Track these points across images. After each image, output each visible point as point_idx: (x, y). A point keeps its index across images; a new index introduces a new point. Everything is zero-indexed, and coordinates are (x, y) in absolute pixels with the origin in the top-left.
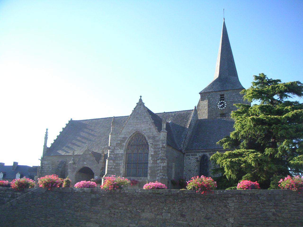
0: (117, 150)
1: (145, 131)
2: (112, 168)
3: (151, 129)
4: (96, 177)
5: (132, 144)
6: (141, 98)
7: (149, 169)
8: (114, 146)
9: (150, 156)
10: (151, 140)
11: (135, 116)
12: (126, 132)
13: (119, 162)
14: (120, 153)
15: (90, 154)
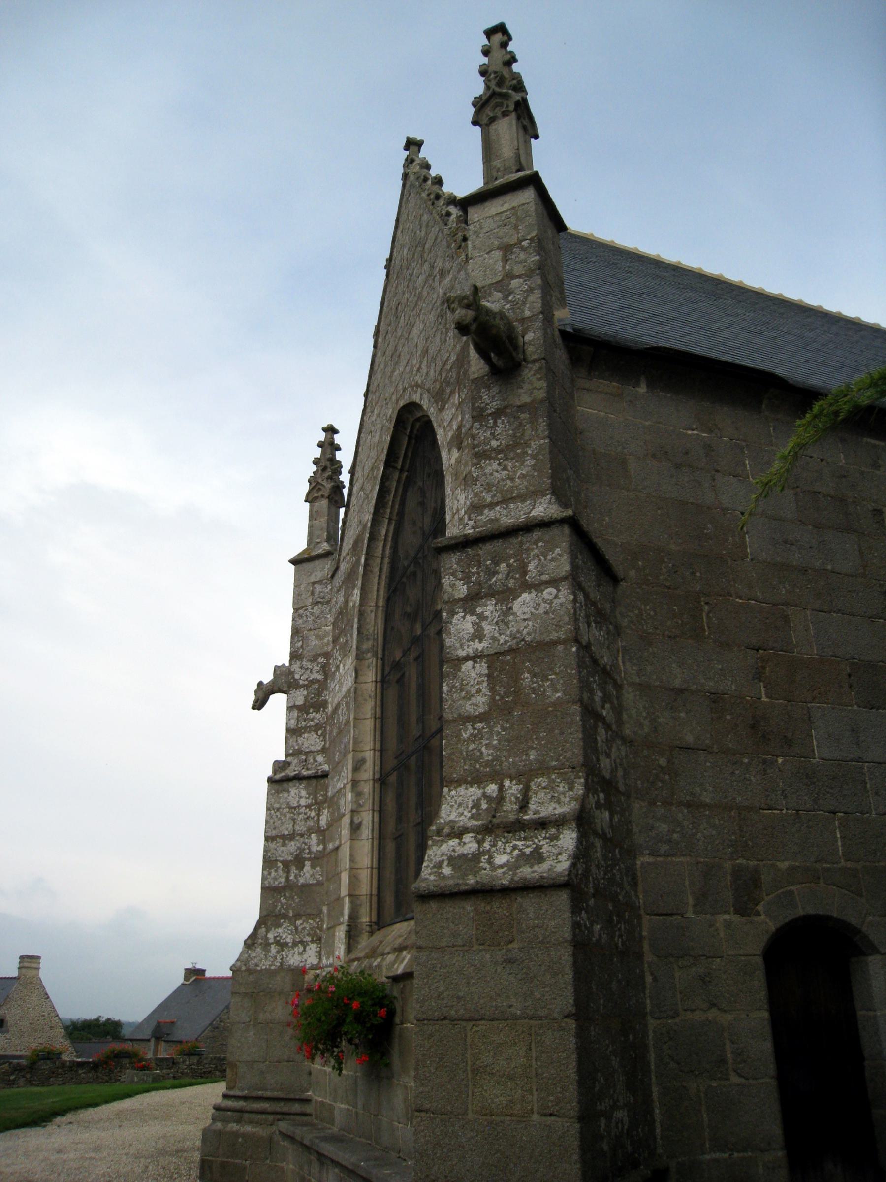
2: (299, 861)
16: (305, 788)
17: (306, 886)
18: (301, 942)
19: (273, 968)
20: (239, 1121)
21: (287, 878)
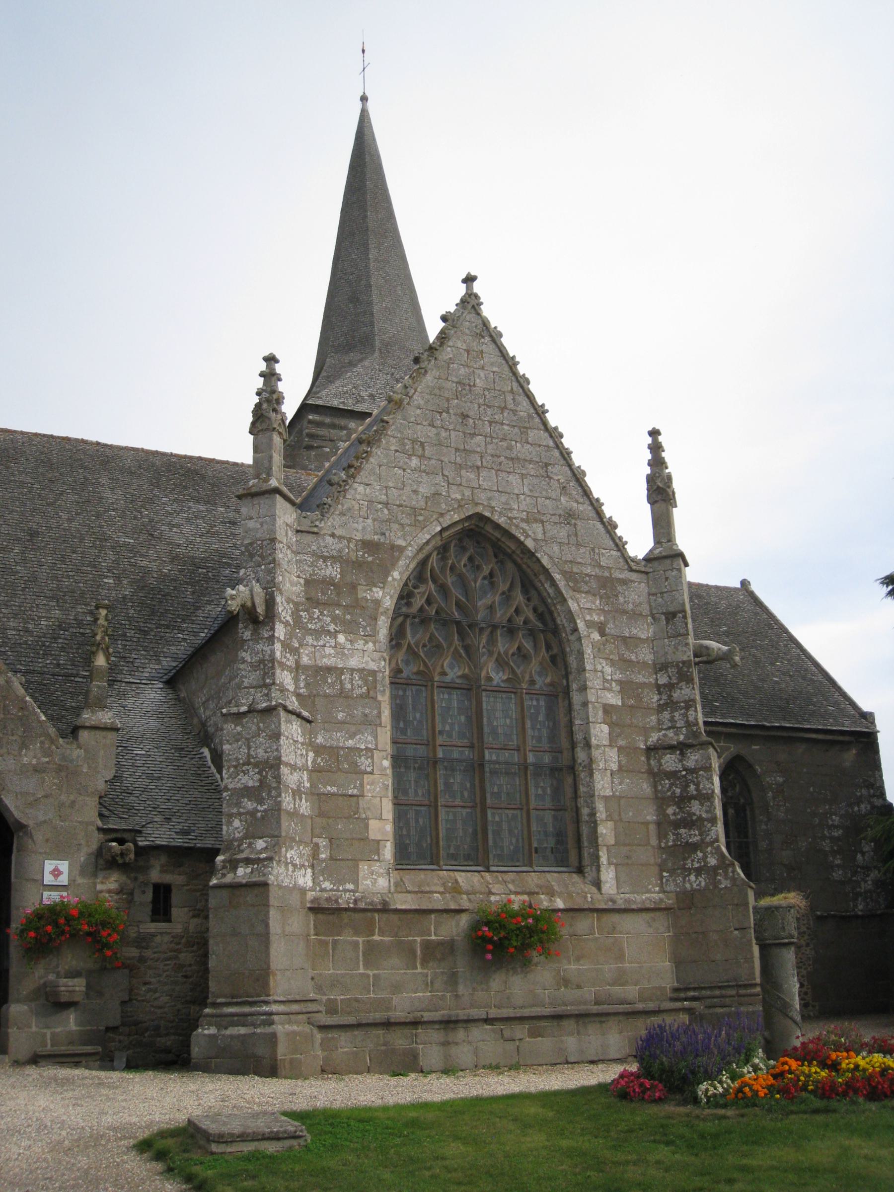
0: (318, 633)
1: (538, 528)
2: (297, 793)
3: (579, 523)
4: (49, 865)
5: (421, 609)
6: (469, 288)
7: (604, 816)
8: (293, 601)
9: (600, 713)
10: (591, 598)
11: (448, 400)
12: (386, 504)
13: (350, 743)
14: (353, 663)
16: (301, 726)
17: (303, 815)
18: (304, 865)
19: (291, 885)
20: (290, 1022)
21: (295, 804)
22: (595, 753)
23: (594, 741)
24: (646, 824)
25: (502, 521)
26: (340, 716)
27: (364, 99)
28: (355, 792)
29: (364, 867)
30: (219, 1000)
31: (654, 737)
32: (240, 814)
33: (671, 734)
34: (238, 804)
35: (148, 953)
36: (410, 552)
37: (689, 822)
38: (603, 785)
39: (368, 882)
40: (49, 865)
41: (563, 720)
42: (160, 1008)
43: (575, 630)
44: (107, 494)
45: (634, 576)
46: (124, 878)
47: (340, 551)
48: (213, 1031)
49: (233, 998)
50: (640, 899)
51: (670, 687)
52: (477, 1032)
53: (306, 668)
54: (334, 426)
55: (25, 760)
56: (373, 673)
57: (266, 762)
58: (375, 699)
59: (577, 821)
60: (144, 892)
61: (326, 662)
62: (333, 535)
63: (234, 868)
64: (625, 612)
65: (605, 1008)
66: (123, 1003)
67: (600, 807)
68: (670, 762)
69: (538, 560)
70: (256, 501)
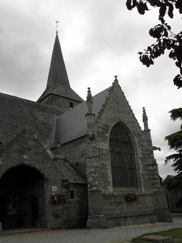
0: (99, 142)
4: (53, 187)
6: (116, 78)
14: (105, 148)
15: (35, 140)
22: (140, 166)
23: (139, 164)
24: (147, 179)
25: (124, 122)
26: (104, 158)
27: (57, 32)
28: (107, 172)
29: (109, 187)
30: (92, 214)
31: (147, 163)
32: (91, 177)
33: (150, 163)
34: (91, 175)
35: (71, 205)
36: (111, 127)
37: (154, 179)
38: (141, 172)
39: (109, 190)
40: (53, 187)
41: (133, 160)
42: (73, 216)
43: (135, 143)
44: (24, 109)
45: (142, 134)
46: (66, 190)
47: (101, 126)
48: (91, 220)
49: (94, 213)
50: (148, 193)
51: (149, 154)
52: (129, 219)
53: (98, 148)
54: (56, 98)
55: (48, 165)
56: (108, 150)
57: (96, 167)
58: (108, 155)
59: (137, 178)
60: (69, 193)
61: (101, 147)
62: (100, 123)
63: (92, 188)
64: (142, 140)
65: (145, 214)
66: (67, 216)
67: (141, 176)
68: (150, 168)
69: (129, 130)
70: (90, 116)
